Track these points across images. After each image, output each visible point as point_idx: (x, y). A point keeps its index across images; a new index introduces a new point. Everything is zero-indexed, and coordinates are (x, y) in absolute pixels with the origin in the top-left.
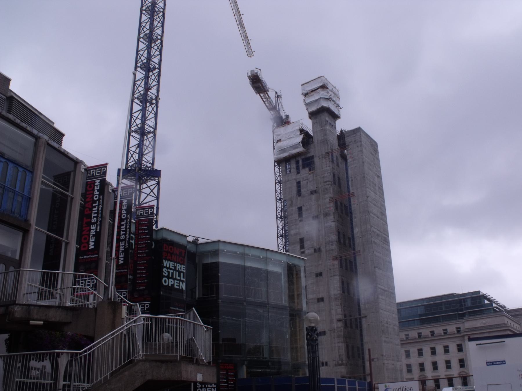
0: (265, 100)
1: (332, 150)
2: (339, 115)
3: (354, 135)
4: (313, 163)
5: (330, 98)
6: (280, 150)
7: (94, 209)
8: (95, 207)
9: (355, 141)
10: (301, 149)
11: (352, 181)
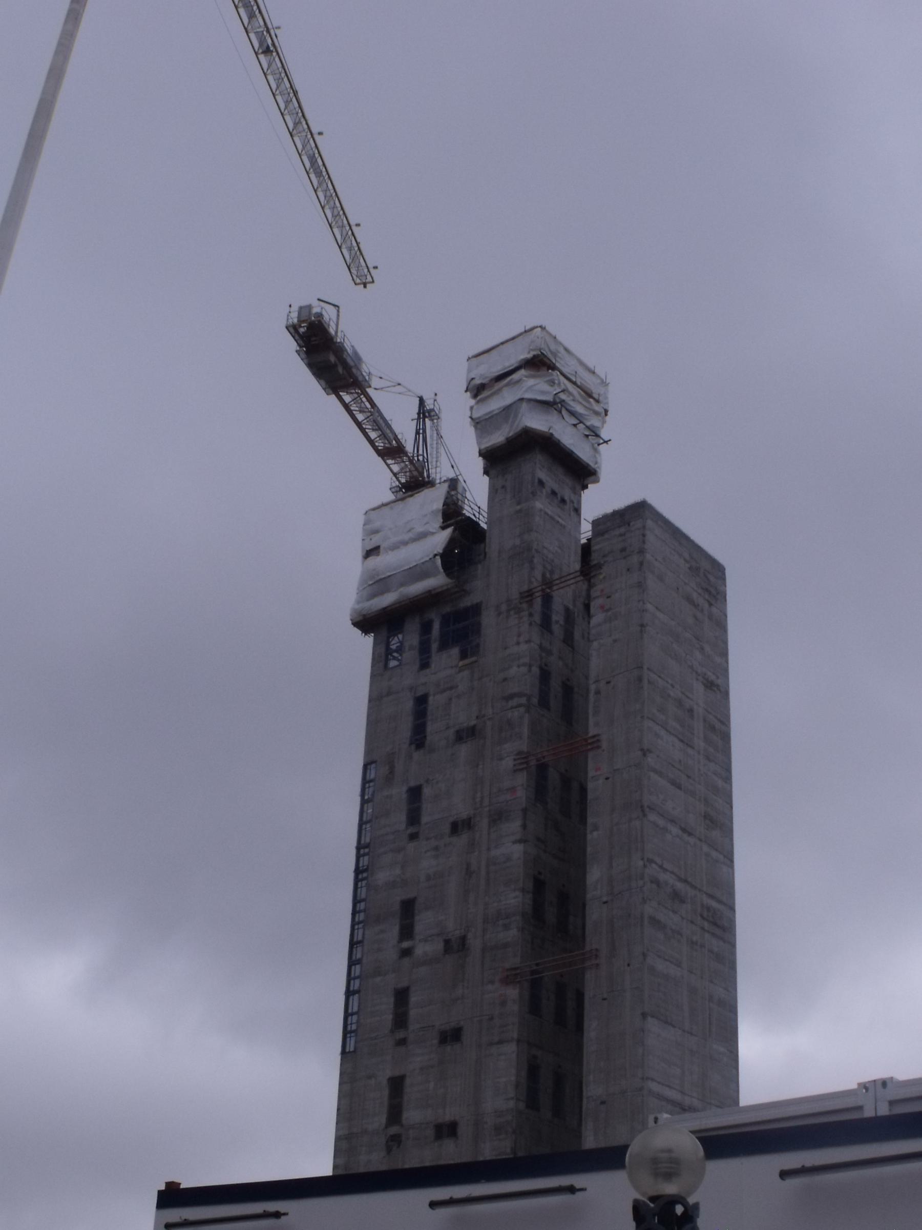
0: (360, 417)
1: (548, 583)
2: (598, 469)
3: (622, 530)
4: (477, 629)
5: (558, 400)
6: (371, 583)
9: (623, 550)
10: (438, 580)
11: (598, 692)
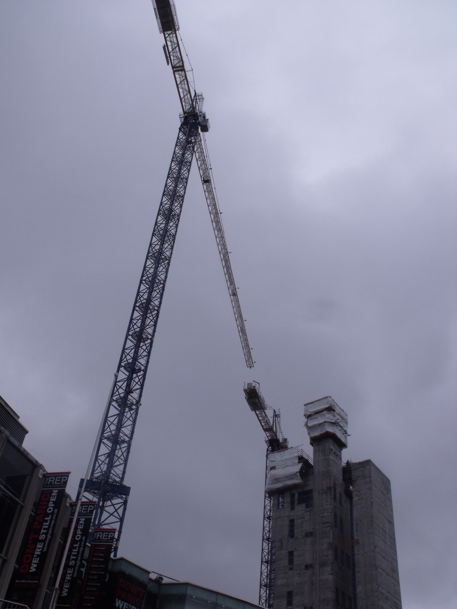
0: (261, 418)
1: (335, 484)
2: (347, 445)
3: (363, 469)
5: (336, 422)
6: (273, 479)
7: (44, 524)
8: (46, 521)
9: (363, 476)
10: (298, 481)
